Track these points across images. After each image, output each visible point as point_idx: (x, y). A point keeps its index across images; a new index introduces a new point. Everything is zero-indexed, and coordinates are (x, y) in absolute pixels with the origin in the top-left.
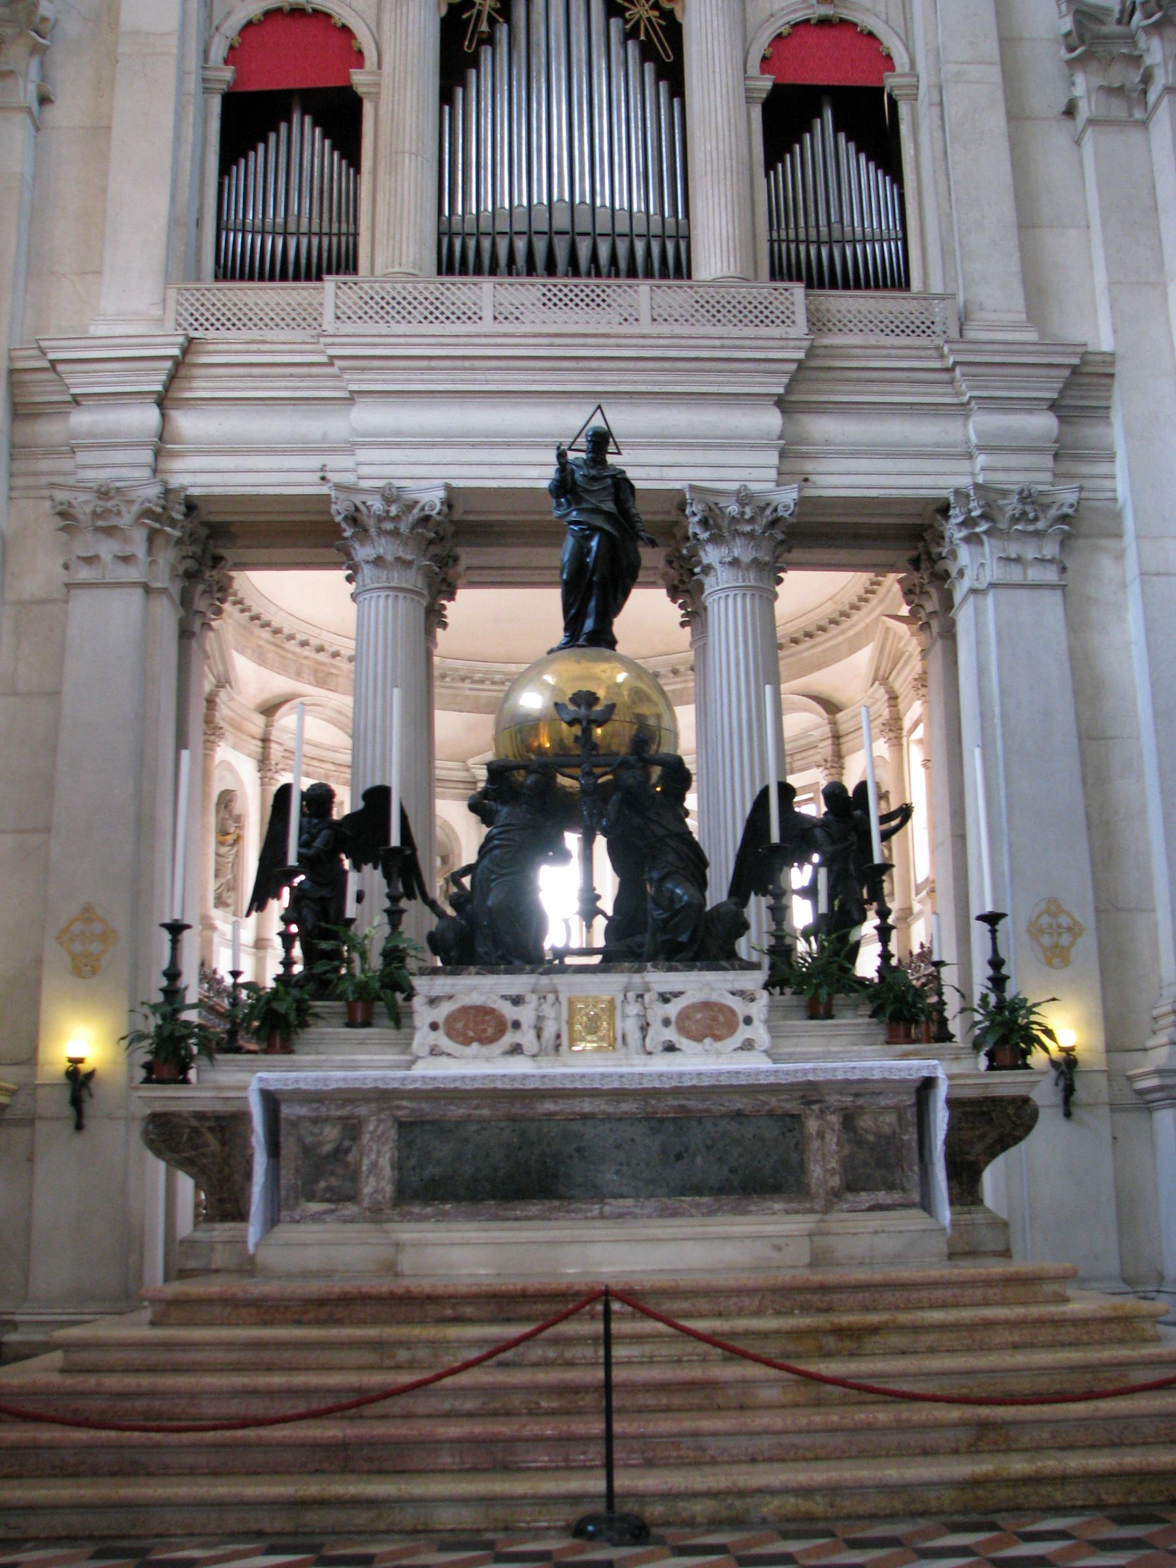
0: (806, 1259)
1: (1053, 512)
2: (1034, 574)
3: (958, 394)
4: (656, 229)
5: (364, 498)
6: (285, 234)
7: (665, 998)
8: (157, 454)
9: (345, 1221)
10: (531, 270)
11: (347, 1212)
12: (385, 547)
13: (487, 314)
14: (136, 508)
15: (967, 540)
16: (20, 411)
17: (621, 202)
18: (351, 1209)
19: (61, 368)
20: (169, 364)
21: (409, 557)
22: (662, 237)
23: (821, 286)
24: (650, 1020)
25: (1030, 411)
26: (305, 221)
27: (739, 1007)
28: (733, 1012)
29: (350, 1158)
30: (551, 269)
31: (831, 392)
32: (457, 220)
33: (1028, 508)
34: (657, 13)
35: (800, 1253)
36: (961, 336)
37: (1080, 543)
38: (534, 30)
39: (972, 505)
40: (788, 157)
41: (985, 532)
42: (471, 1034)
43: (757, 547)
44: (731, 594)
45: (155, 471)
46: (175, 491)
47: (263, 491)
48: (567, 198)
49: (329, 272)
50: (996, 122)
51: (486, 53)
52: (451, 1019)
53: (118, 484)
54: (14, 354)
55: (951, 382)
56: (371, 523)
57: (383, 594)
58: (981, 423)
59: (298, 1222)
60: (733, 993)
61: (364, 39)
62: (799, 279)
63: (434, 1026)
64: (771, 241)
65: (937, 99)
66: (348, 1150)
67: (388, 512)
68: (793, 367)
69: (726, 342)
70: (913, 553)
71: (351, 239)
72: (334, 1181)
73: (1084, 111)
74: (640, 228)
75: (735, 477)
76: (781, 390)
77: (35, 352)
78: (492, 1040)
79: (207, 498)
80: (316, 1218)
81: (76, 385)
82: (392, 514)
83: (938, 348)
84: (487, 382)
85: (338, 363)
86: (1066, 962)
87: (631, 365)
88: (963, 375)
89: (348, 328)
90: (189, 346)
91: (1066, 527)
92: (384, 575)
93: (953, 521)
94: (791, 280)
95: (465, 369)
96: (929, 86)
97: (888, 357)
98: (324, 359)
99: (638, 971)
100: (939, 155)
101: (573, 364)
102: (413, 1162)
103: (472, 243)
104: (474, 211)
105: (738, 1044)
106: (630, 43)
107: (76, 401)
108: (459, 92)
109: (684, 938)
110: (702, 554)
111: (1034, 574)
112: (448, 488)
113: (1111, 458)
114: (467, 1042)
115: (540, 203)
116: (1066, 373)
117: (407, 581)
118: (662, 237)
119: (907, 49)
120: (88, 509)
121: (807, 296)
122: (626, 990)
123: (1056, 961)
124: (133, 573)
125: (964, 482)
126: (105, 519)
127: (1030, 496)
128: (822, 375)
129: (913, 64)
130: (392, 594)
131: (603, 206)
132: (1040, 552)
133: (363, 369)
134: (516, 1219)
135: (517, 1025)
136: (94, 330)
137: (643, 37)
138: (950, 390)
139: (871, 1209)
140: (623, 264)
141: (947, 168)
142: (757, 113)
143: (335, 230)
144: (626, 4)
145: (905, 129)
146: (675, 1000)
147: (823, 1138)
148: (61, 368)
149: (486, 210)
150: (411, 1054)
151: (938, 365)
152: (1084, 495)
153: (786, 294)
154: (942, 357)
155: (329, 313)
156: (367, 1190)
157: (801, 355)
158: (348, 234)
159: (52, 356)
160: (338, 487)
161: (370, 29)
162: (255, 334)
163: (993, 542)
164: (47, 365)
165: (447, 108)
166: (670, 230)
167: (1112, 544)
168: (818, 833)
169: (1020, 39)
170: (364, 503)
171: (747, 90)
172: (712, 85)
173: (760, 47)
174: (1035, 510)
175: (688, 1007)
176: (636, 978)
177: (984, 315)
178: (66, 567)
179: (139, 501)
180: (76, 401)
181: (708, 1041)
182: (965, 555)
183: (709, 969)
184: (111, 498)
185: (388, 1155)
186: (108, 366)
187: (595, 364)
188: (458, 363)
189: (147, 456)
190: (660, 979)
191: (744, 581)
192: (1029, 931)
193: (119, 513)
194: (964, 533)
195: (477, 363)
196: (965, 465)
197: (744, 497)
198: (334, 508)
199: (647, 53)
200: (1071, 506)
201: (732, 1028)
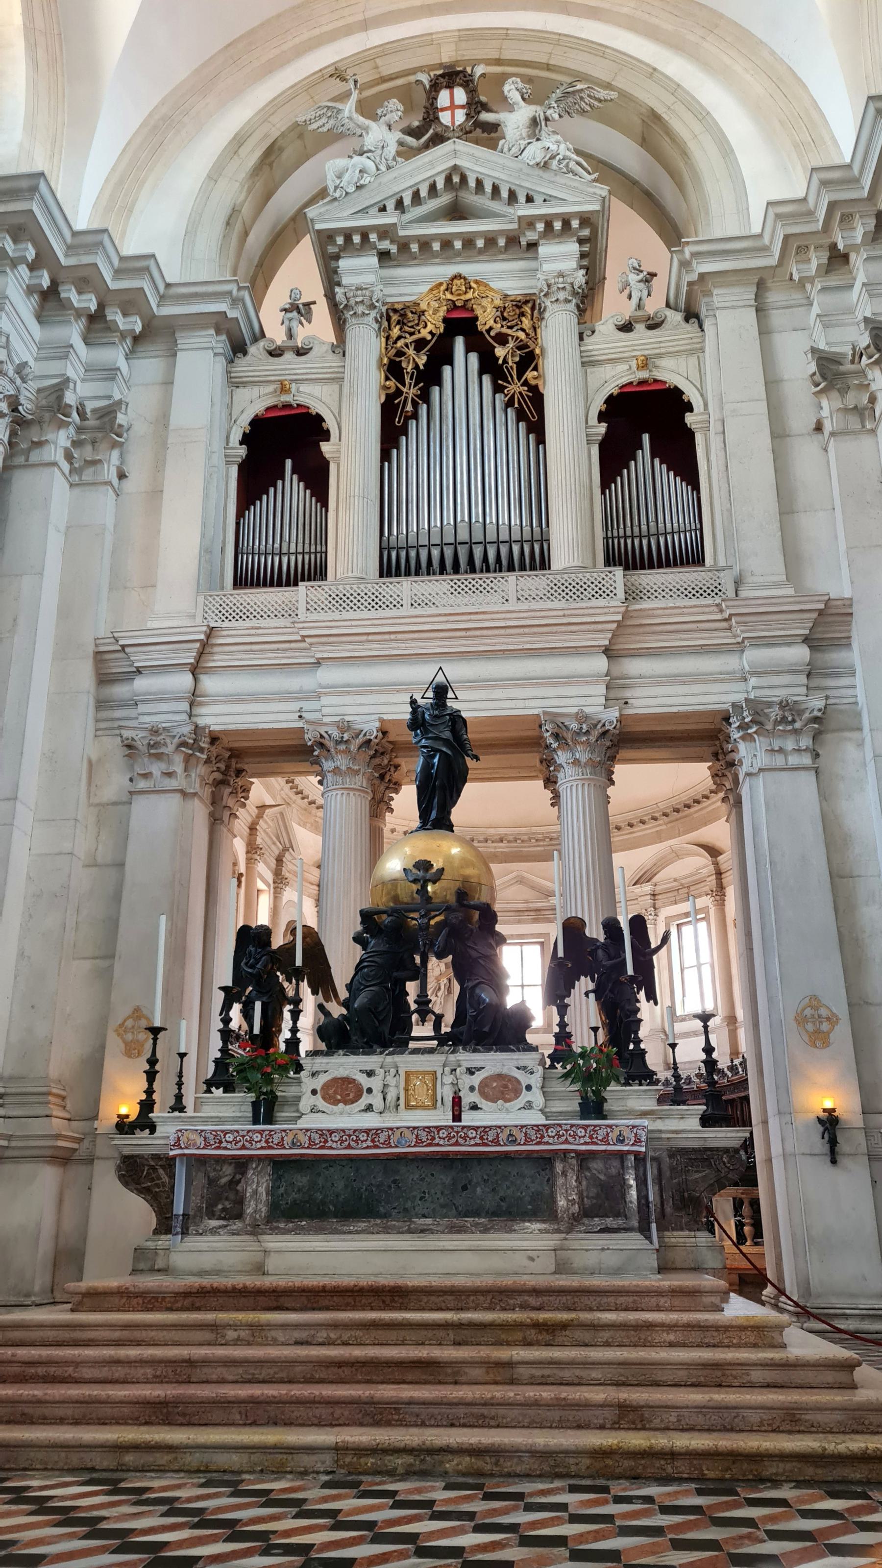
0: (552, 1268)
1: (807, 715)
2: (794, 760)
3: (735, 636)
4: (527, 536)
5: (326, 728)
6: (281, 554)
7: (471, 1072)
8: (191, 705)
9: (234, 1234)
10: (443, 570)
11: (235, 1227)
12: (342, 762)
13: (406, 602)
14: (176, 741)
15: (743, 738)
16: (104, 679)
17: (504, 519)
18: (238, 1225)
19: (127, 650)
20: (198, 645)
21: (356, 768)
22: (532, 542)
23: (635, 568)
24: (460, 1086)
25: (789, 644)
26: (293, 546)
27: (524, 1079)
28: (519, 1082)
29: (239, 1188)
30: (456, 569)
31: (640, 642)
32: (393, 539)
33: (786, 714)
34: (526, 388)
35: (547, 1263)
36: (737, 596)
37: (828, 737)
38: (444, 407)
39: (745, 714)
40: (619, 478)
41: (755, 732)
42: (339, 1097)
43: (592, 752)
44: (575, 784)
45: (190, 716)
46: (204, 728)
47: (261, 726)
48: (466, 519)
49: (303, 580)
50: (764, 440)
51: (412, 424)
52: (326, 1086)
53: (164, 725)
54: (98, 642)
55: (730, 628)
56: (330, 745)
57: (340, 792)
58: (754, 656)
59: (201, 1234)
60: (518, 1068)
61: (330, 423)
62: (620, 565)
63: (314, 1092)
64: (607, 538)
65: (722, 429)
66: (239, 1181)
67: (342, 737)
68: (615, 625)
69: (566, 612)
70: (712, 749)
71: (323, 555)
72: (228, 1205)
73: (828, 427)
74: (516, 536)
75: (576, 704)
76: (607, 643)
77: (112, 640)
78: (353, 1102)
79: (226, 732)
80: (214, 1231)
81: (139, 661)
82: (345, 739)
83: (717, 605)
84: (406, 648)
85: (307, 640)
86: (826, 1044)
87: (502, 632)
88: (737, 623)
89: (314, 616)
90: (211, 632)
91: (816, 726)
92: (340, 779)
93: (734, 726)
94: (615, 565)
95: (392, 640)
96: (715, 421)
97: (682, 614)
98: (300, 638)
99: (452, 1053)
100: (723, 468)
101: (463, 633)
102: (282, 1190)
103: (403, 554)
104: (405, 532)
105: (363, 1108)
106: (509, 410)
107: (139, 671)
108: (394, 452)
109: (486, 1029)
110: (556, 756)
111: (794, 760)
112: (382, 721)
113: (853, 674)
114: (335, 1102)
115: (449, 524)
116: (815, 615)
117: (355, 784)
118: (532, 542)
119: (702, 395)
120: (145, 742)
121: (625, 576)
122: (444, 1066)
123: (818, 1043)
124: (173, 784)
125: (739, 698)
126: (156, 748)
127: (788, 704)
128: (637, 630)
129: (706, 405)
130: (345, 792)
131: (491, 523)
132: (798, 744)
133: (323, 644)
134: (350, 1233)
135: (370, 1091)
136: (150, 625)
137: (516, 405)
138: (729, 634)
139: (601, 1231)
140: (504, 562)
141: (728, 477)
142: (595, 450)
143: (313, 550)
144: (505, 384)
146: (477, 1073)
147: (566, 1176)
148: (127, 650)
149: (412, 531)
150: (298, 1111)
151: (719, 617)
152: (830, 701)
153: (610, 575)
154: (721, 611)
155: (302, 606)
156: (249, 1211)
157: (619, 618)
158: (321, 552)
159: (121, 642)
160: (308, 722)
161: (334, 415)
162: (254, 623)
163: (761, 738)
164: (120, 648)
165: (386, 464)
166: (537, 536)
167: (855, 735)
168: (600, 952)
169: (782, 381)
170: (326, 732)
171: (587, 435)
172: (562, 434)
173: (598, 404)
174: (793, 715)
175: (486, 1078)
176: (452, 1058)
177: (755, 579)
178: (131, 780)
179: (178, 735)
180: (139, 671)
181: (500, 1102)
182: (743, 749)
183: (502, 1051)
184: (161, 734)
185: (264, 1185)
186: (158, 647)
187: (478, 633)
188: (387, 637)
189: (185, 706)
190: (466, 1058)
191: (583, 775)
192: (796, 1020)
193: (165, 744)
194: (741, 733)
195: (399, 636)
196: (741, 686)
197: (581, 717)
198: (306, 736)
199: (521, 416)
200: (820, 710)
201: (517, 1093)
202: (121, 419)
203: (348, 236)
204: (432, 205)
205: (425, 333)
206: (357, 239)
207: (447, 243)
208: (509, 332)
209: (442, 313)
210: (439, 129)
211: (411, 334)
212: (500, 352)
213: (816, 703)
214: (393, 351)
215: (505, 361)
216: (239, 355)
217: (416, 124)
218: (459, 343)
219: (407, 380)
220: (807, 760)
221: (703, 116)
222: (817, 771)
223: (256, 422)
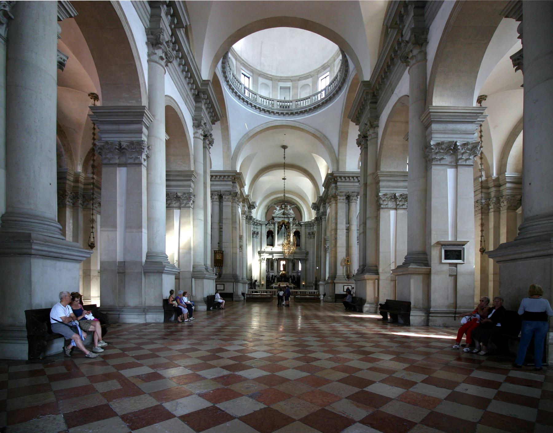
58: (302, 255)
223: (268, 231)
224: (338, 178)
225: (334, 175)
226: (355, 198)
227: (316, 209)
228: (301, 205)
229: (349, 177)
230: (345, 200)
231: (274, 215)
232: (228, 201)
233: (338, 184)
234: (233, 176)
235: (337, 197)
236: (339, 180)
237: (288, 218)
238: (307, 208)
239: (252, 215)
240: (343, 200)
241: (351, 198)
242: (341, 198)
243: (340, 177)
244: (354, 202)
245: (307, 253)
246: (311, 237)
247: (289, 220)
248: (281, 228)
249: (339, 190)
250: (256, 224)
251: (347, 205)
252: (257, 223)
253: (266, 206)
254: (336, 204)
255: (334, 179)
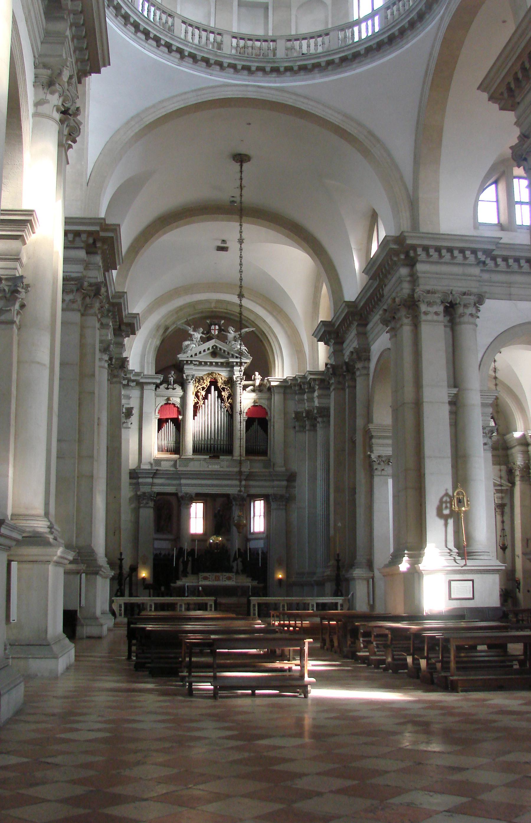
2: (281, 507)
7: (225, 576)
73: (297, 429)
145: (269, 426)
190: (224, 574)
199: (227, 411)
202: (133, 412)
203: (187, 361)
204: (207, 352)
205: (204, 386)
206: (189, 362)
207: (211, 363)
208: (225, 387)
209: (209, 380)
210: (211, 335)
211: (201, 385)
212: (223, 393)
213: (287, 495)
214: (196, 390)
215: (224, 397)
216: (158, 388)
217: (205, 332)
218: (213, 387)
219: (200, 399)
220: (284, 507)
221: (276, 337)
222: (286, 509)
224: (419, 251)
225: (409, 242)
226: (471, 310)
227: (333, 341)
228: (270, 327)
229: (450, 250)
230: (442, 315)
231: (182, 357)
232: (73, 310)
233: (420, 267)
234: (90, 233)
235: (418, 306)
236: (422, 256)
237: (230, 366)
238: (289, 337)
239: (125, 355)
240: (436, 313)
241: (461, 310)
242: (429, 309)
243: (426, 249)
244: (469, 323)
245: (291, 478)
246: (304, 427)
247: (232, 372)
248: (206, 398)
249: (422, 287)
250: (125, 382)
251: (448, 330)
252: (129, 380)
253: (158, 327)
254: (416, 326)
255: (407, 254)
